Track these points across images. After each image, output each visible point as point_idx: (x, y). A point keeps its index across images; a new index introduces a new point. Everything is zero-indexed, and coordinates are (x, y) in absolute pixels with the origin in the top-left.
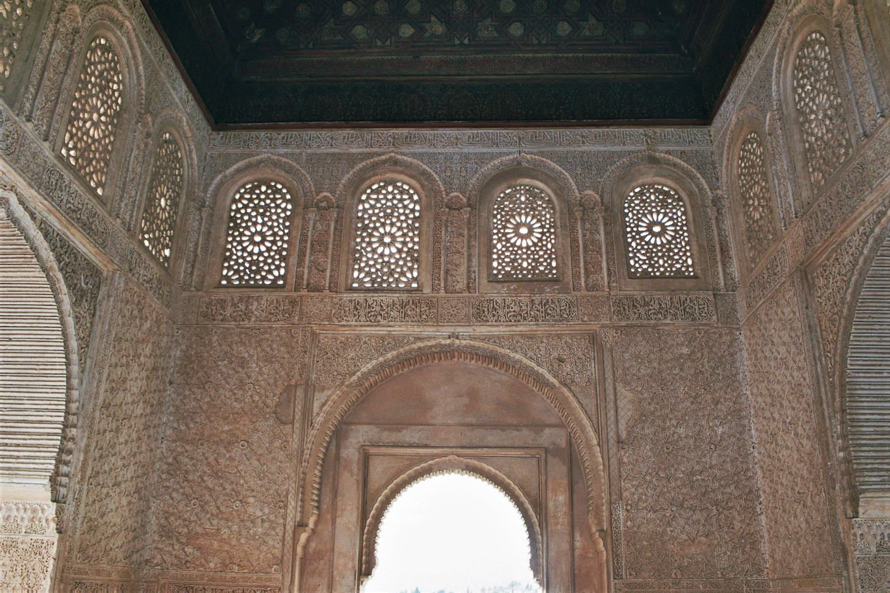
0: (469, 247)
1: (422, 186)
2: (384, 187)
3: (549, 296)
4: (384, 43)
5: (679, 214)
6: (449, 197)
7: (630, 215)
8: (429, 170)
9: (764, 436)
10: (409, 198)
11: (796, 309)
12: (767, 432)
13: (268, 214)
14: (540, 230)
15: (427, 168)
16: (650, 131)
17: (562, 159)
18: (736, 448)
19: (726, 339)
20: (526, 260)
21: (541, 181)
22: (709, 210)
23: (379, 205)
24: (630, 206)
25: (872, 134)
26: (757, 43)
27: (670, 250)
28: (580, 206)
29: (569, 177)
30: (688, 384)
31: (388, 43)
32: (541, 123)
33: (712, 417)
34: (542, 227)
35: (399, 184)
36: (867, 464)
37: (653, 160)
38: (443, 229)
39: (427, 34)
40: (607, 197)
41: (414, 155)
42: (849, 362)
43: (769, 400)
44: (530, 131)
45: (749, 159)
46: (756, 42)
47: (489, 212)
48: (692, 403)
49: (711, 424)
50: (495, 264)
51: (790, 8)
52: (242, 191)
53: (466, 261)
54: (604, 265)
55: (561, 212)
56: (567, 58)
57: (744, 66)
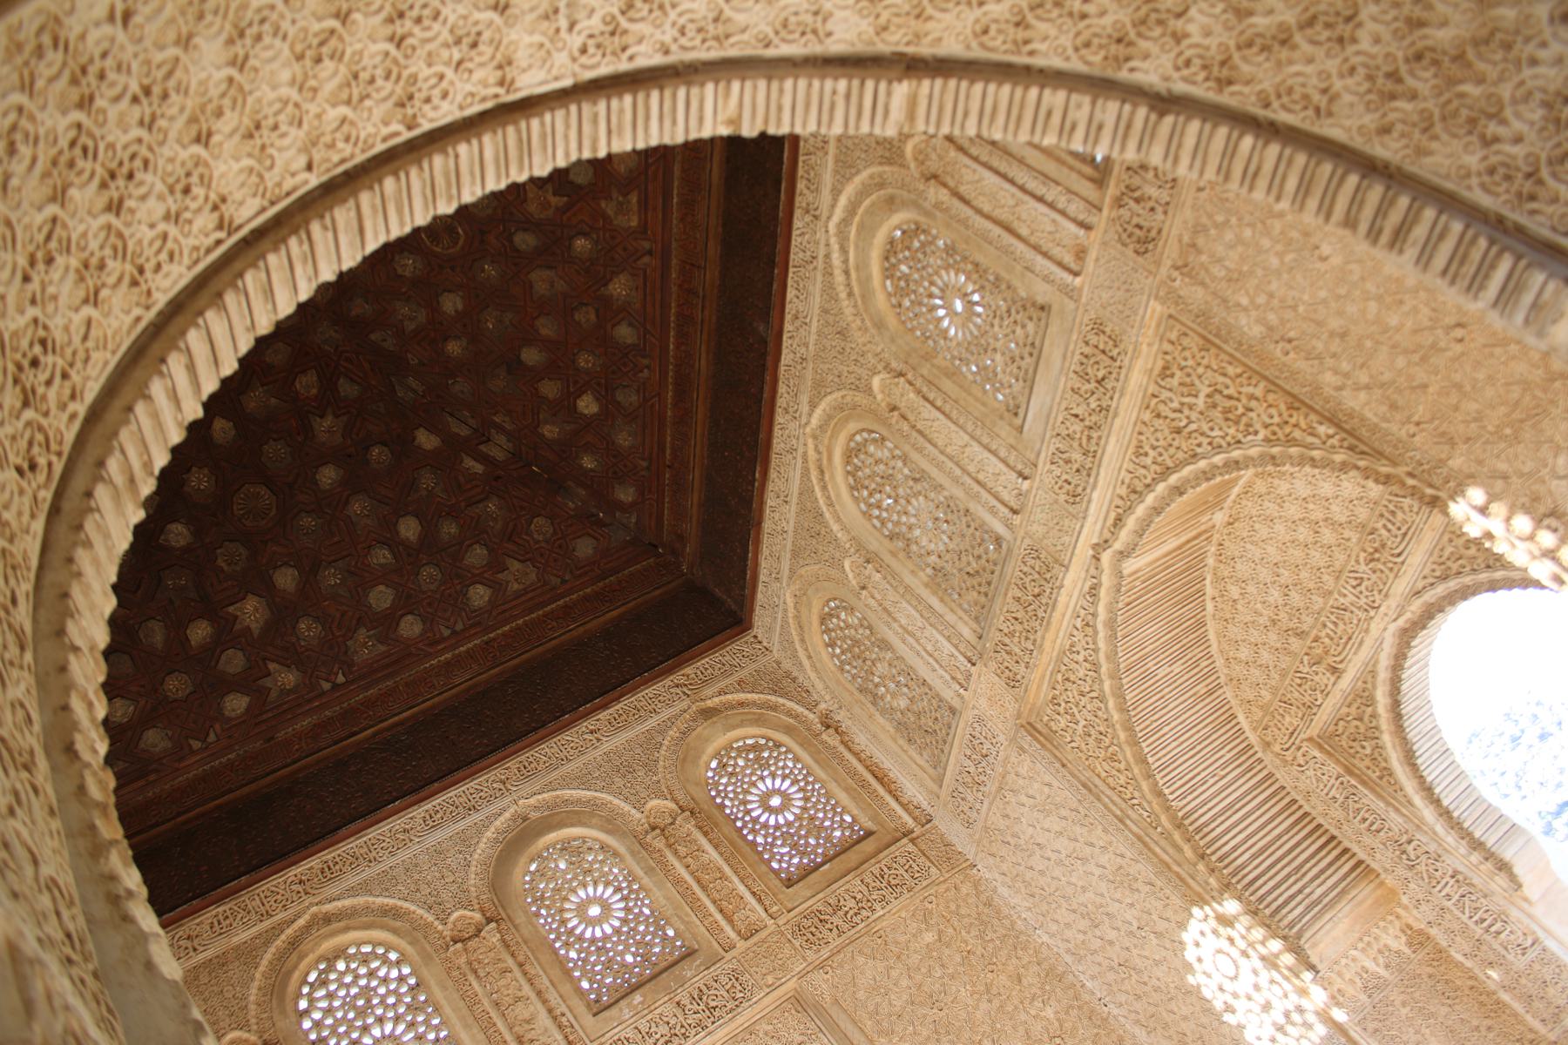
0: (531, 982)
1: (395, 931)
2: (331, 967)
3: (699, 981)
4: (204, 741)
5: (790, 764)
6: (450, 926)
7: (727, 803)
8: (391, 902)
9: (1111, 976)
10: (384, 963)
11: (1048, 778)
12: (1112, 968)
13: (375, 1001)
14: (618, 896)
15: (386, 901)
16: (677, 677)
17: (583, 781)
18: (1085, 1022)
19: (965, 889)
20: (627, 949)
21: (572, 825)
22: (824, 736)
23: (336, 1003)
24: (719, 792)
25: (1023, 505)
26: (775, 484)
27: (812, 818)
28: (653, 829)
29: (610, 798)
30: (966, 978)
31: (212, 737)
32: (519, 745)
33: (1027, 1002)
34: (618, 889)
35: (352, 951)
36: (1275, 899)
37: (708, 713)
38: (471, 978)
39: (274, 694)
40: (680, 795)
41: (352, 892)
42: (1166, 791)
43: (1084, 924)
44: (513, 764)
45: (843, 639)
46: (770, 486)
47: (526, 912)
48: (990, 1001)
49: (1033, 1012)
50: (585, 985)
51: (804, 420)
52: (306, 990)
53: (539, 1006)
54: (742, 888)
55: (633, 853)
56: (504, 635)
57: (767, 526)
